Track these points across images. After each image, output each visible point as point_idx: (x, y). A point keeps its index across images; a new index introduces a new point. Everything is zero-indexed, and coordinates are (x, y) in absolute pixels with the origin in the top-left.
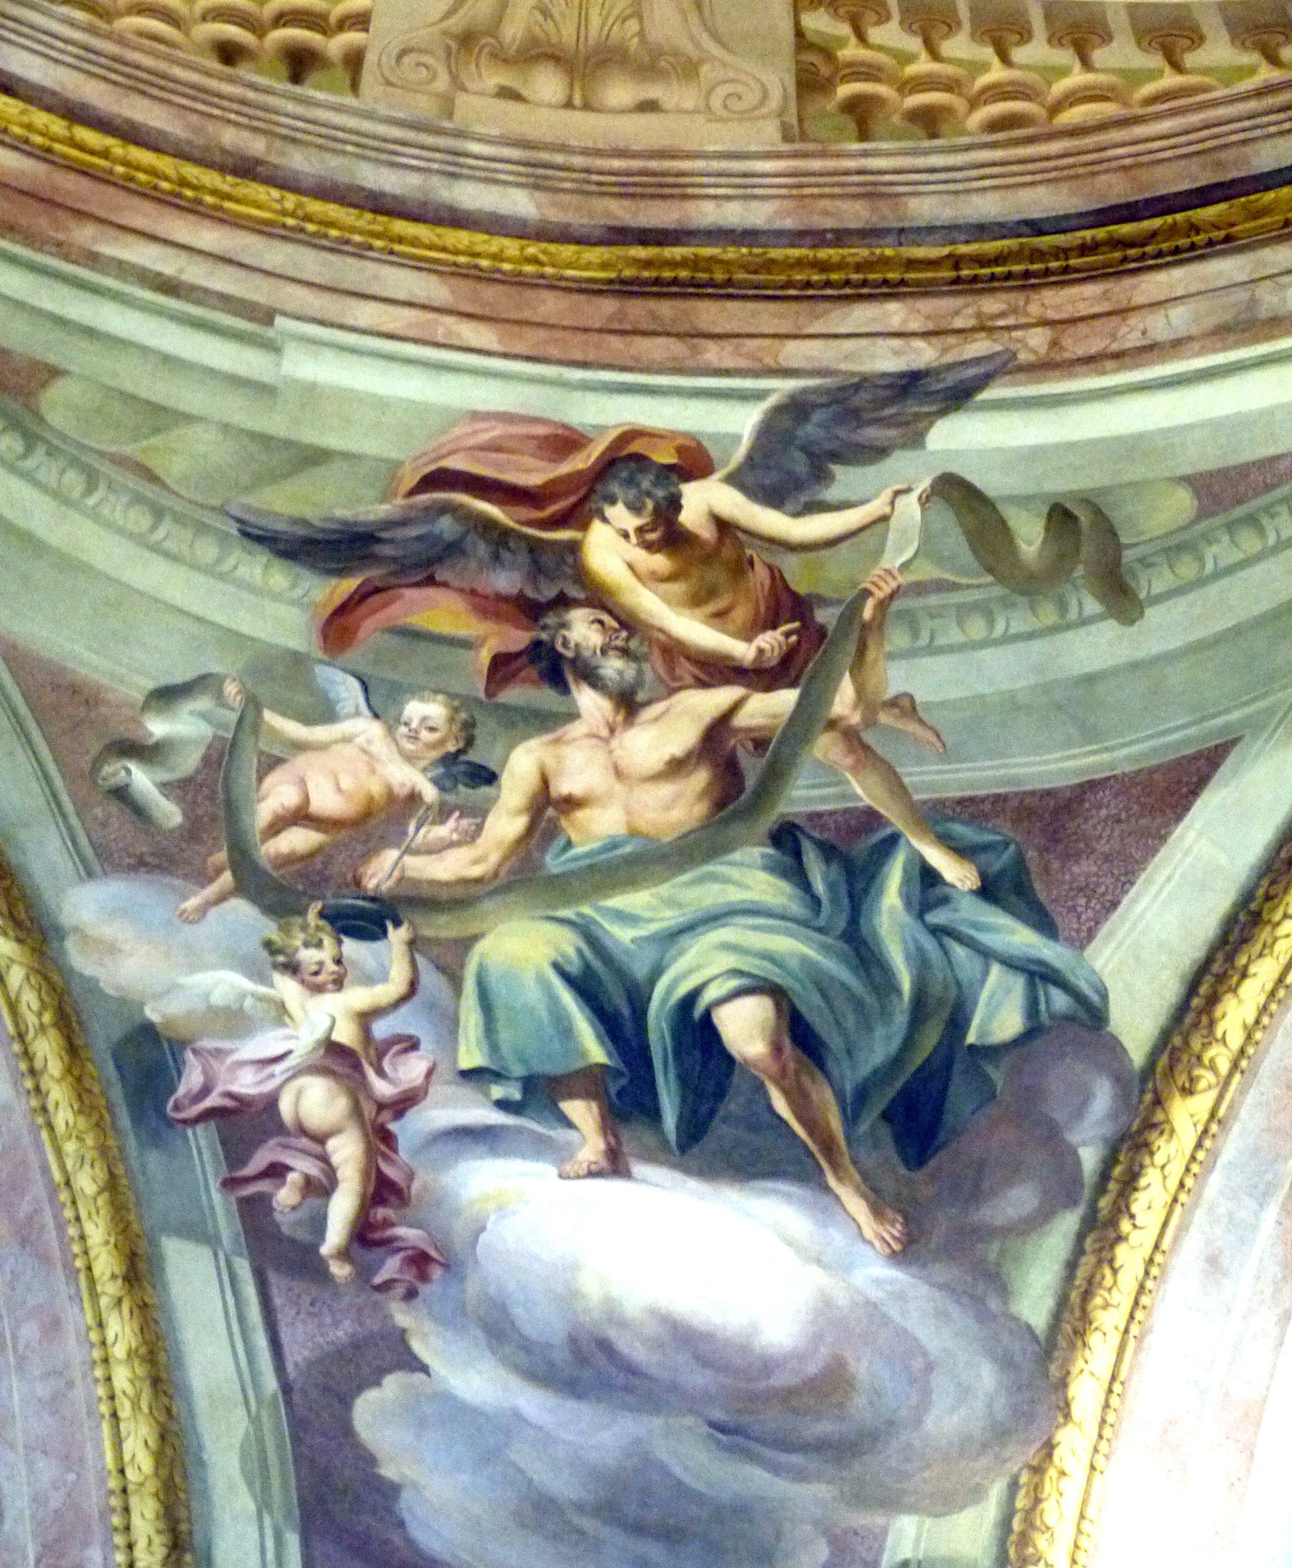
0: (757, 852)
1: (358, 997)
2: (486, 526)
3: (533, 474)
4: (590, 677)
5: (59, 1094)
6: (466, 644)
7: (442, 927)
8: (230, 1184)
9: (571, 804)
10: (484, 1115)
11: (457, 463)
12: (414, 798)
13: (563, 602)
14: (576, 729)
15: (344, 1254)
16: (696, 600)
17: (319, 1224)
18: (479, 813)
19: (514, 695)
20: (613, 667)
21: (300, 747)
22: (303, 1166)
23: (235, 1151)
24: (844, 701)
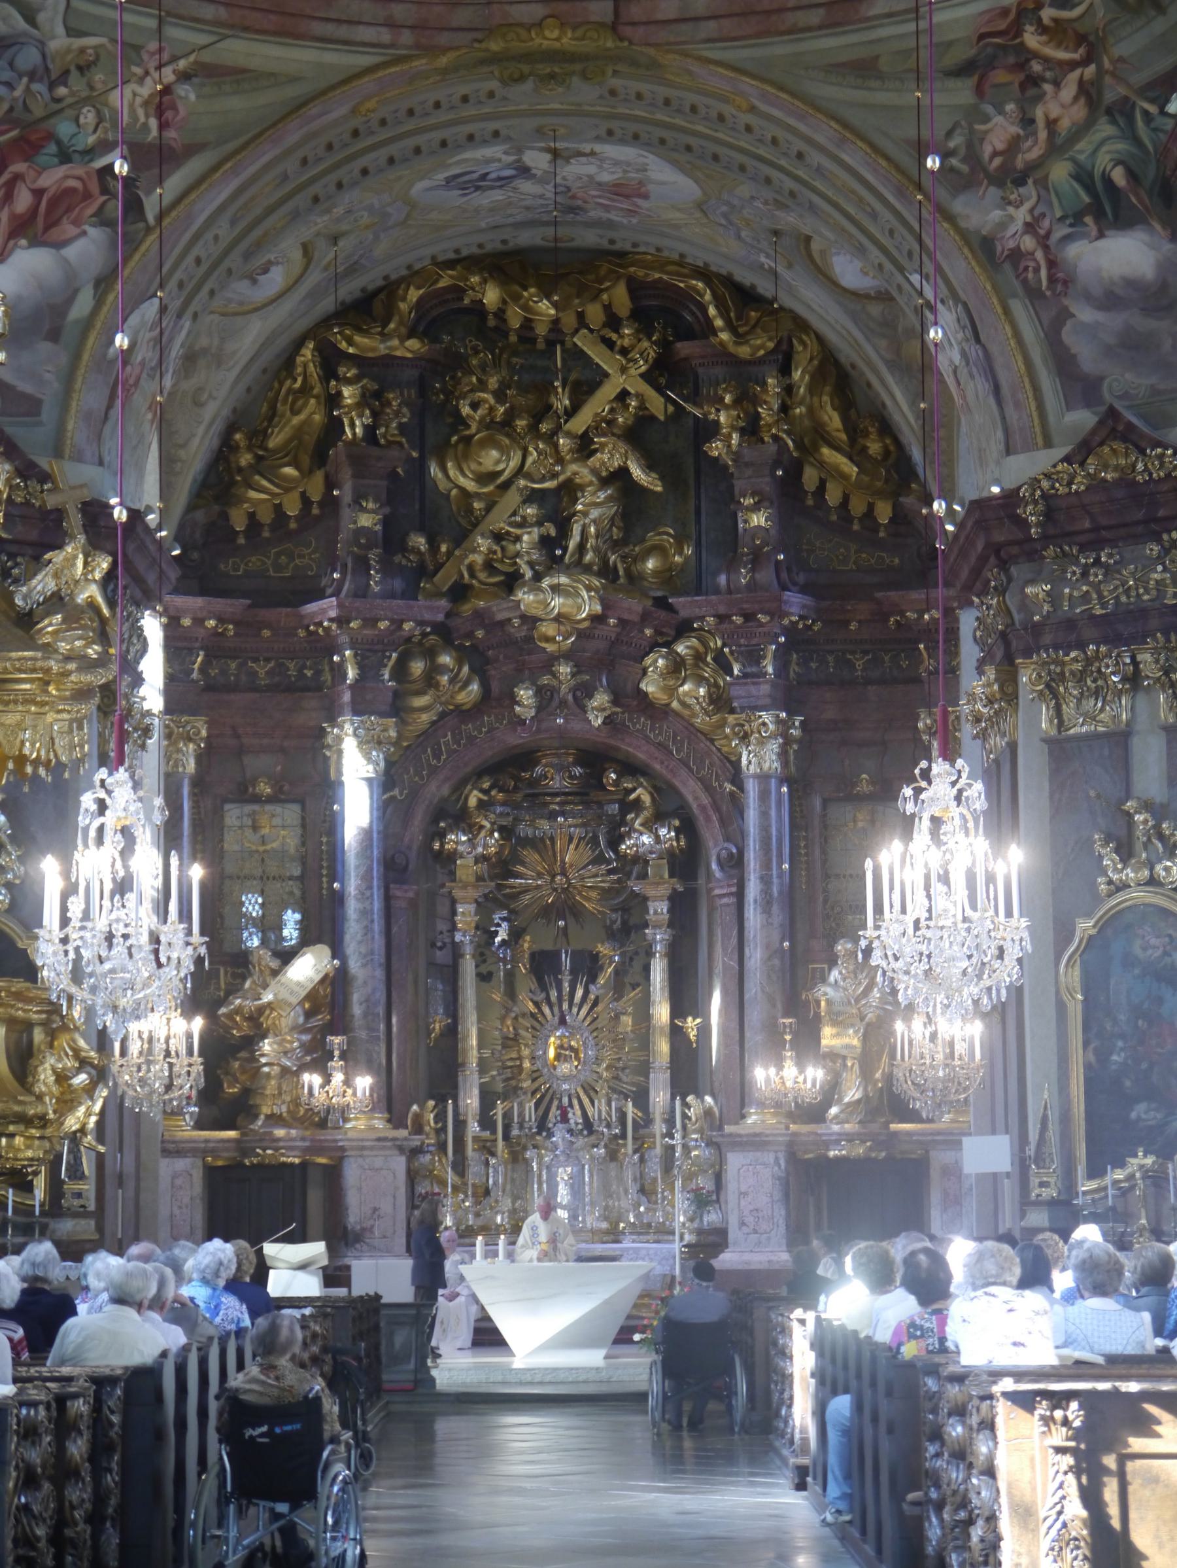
0: (1104, 119)
1: (1027, 205)
2: (998, 45)
3: (1002, 25)
4: (1044, 80)
5: (974, 263)
6: (1011, 83)
7: (1039, 174)
8: (1017, 277)
9: (1055, 121)
10: (1067, 231)
11: (984, 30)
12: (1018, 136)
13: (1028, 60)
14: (1048, 97)
15: (1048, 288)
16: (1059, 45)
17: (1040, 281)
18: (1035, 133)
19: (1032, 92)
20: (1048, 74)
21: (986, 132)
22: (1032, 264)
23: (1015, 266)
24: (1107, 64)
